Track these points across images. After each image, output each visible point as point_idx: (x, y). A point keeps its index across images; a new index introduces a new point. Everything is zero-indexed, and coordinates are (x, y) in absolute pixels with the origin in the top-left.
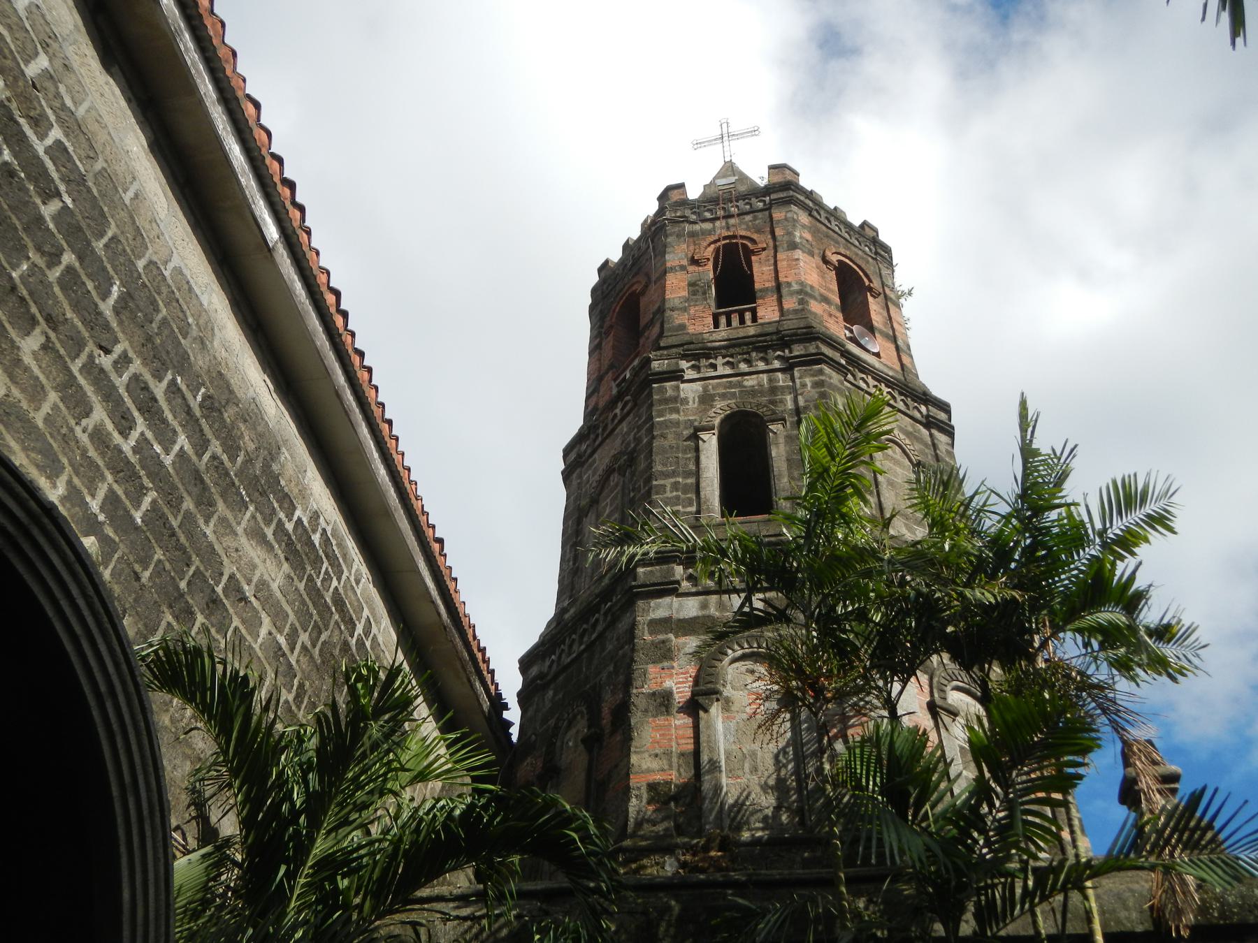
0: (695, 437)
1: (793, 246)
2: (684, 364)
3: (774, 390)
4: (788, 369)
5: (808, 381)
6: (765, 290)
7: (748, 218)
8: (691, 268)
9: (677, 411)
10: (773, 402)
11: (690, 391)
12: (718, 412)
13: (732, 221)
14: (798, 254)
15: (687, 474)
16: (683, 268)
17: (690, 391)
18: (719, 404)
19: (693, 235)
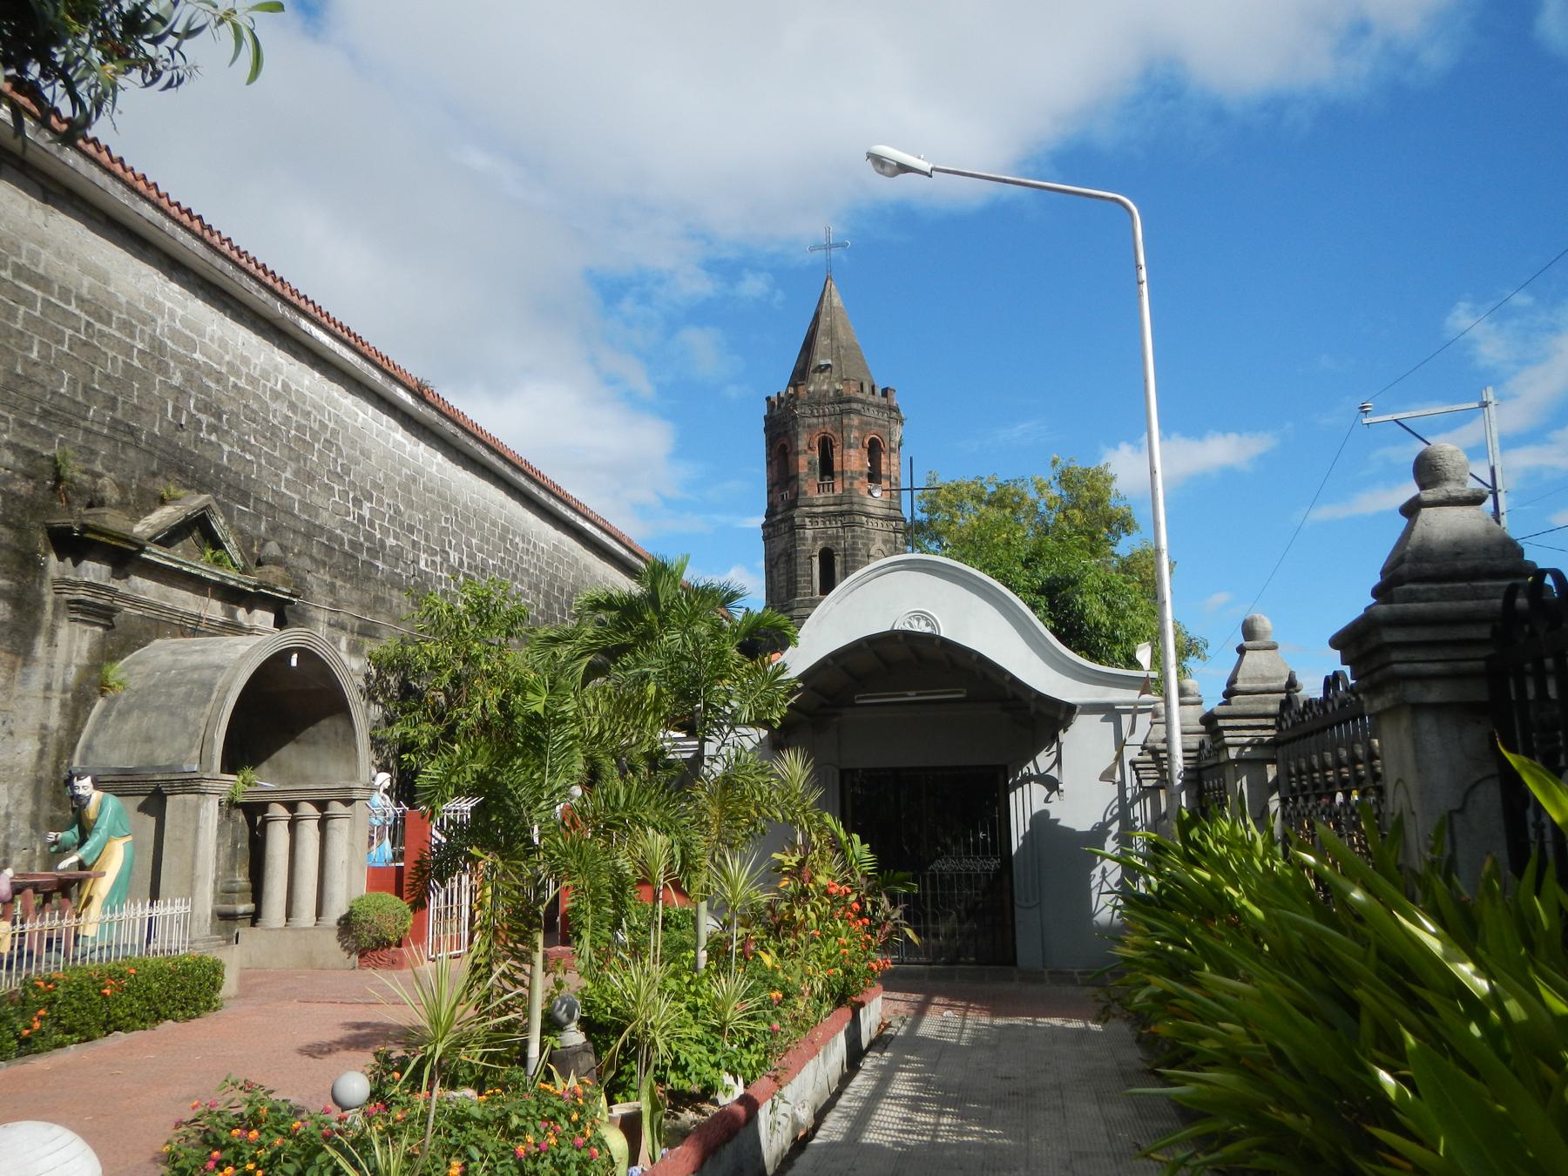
0: (810, 558)
1: (850, 447)
2: (807, 520)
3: (838, 537)
4: (843, 527)
5: (850, 534)
6: (837, 472)
7: (833, 418)
8: (809, 452)
9: (804, 545)
10: (837, 543)
11: (809, 533)
12: (820, 544)
13: (826, 419)
14: (852, 452)
15: (808, 575)
16: (806, 452)
17: (809, 533)
18: (819, 543)
19: (809, 426)
